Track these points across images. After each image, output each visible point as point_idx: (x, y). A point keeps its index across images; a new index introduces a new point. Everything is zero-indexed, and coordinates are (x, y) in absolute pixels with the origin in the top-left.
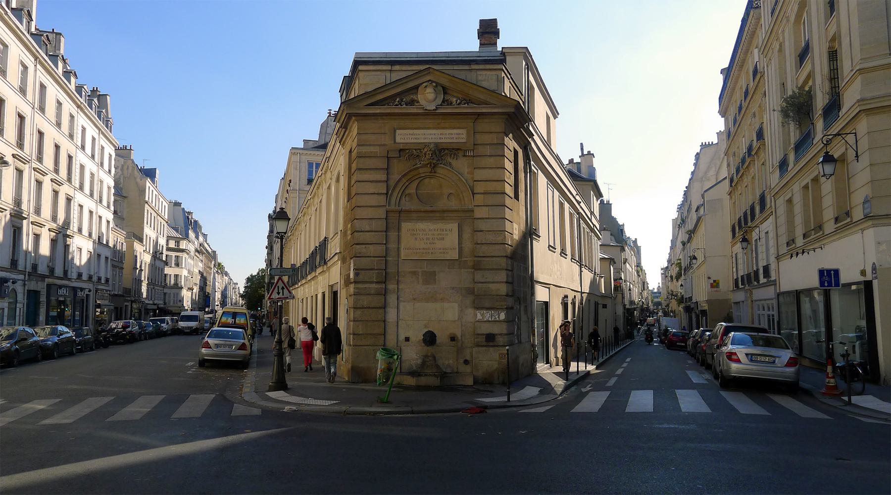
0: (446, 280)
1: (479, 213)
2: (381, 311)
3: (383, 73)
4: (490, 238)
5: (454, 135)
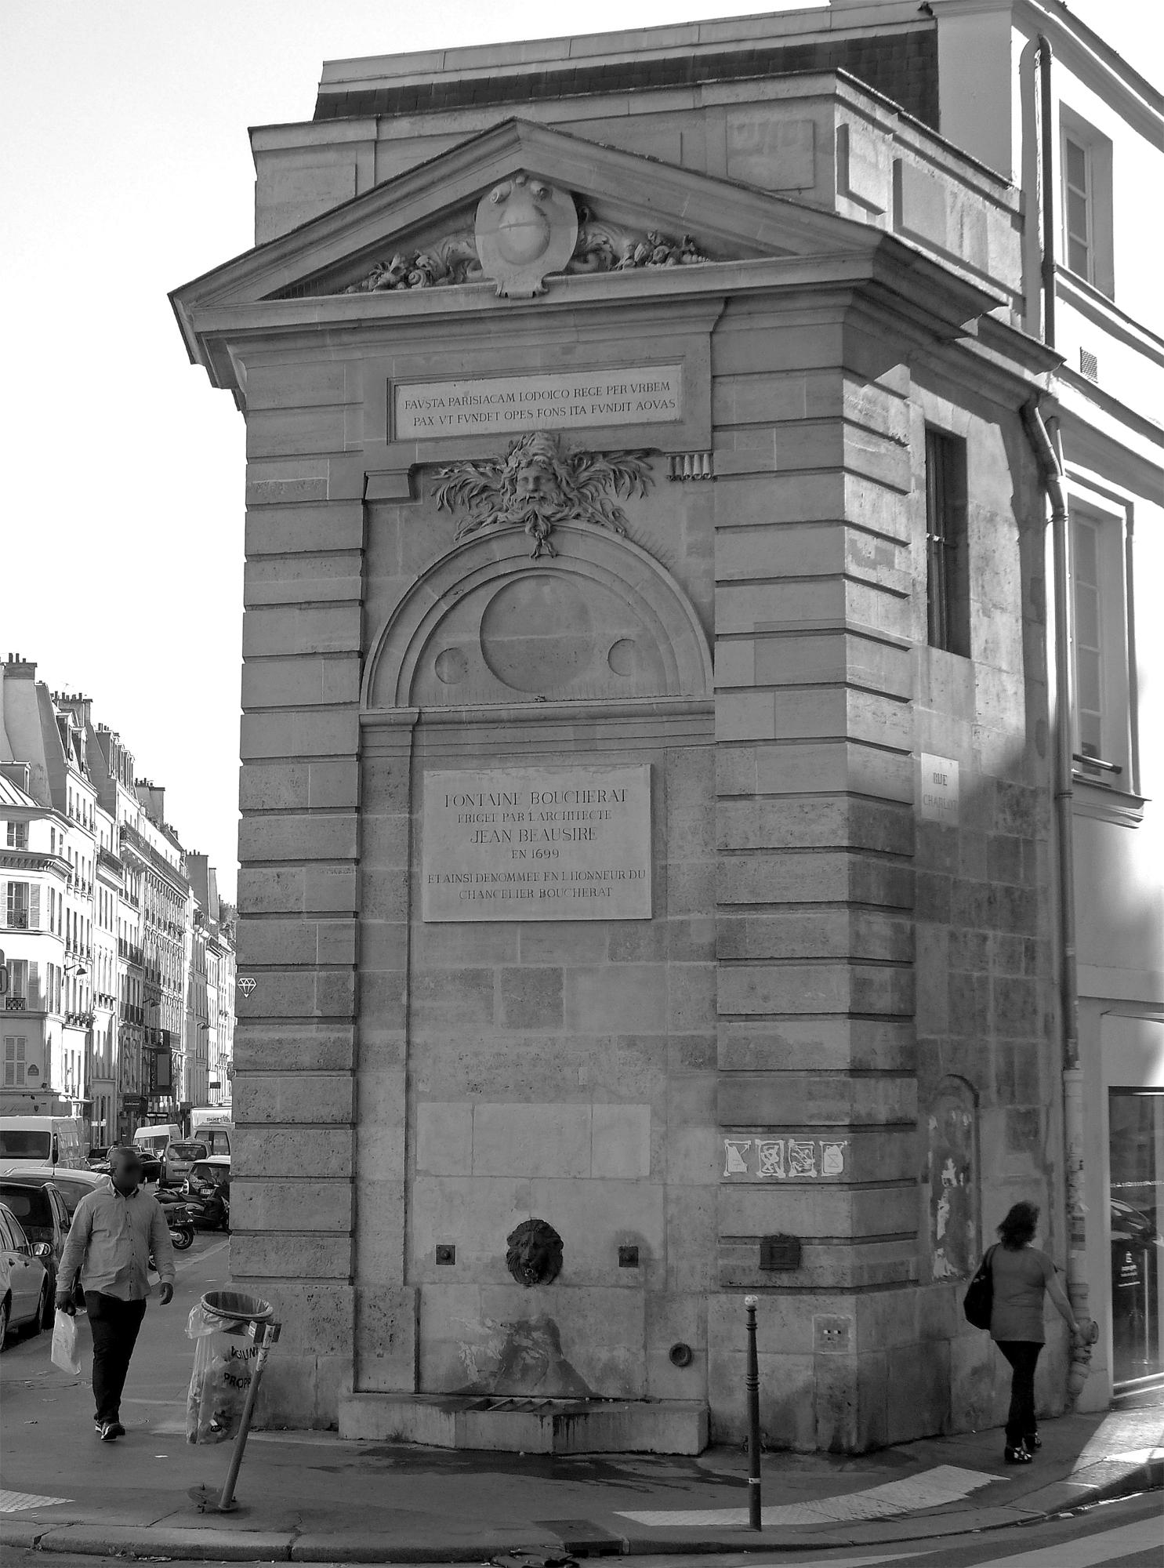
2: (343, 1137)
3: (350, 156)
5: (625, 392)
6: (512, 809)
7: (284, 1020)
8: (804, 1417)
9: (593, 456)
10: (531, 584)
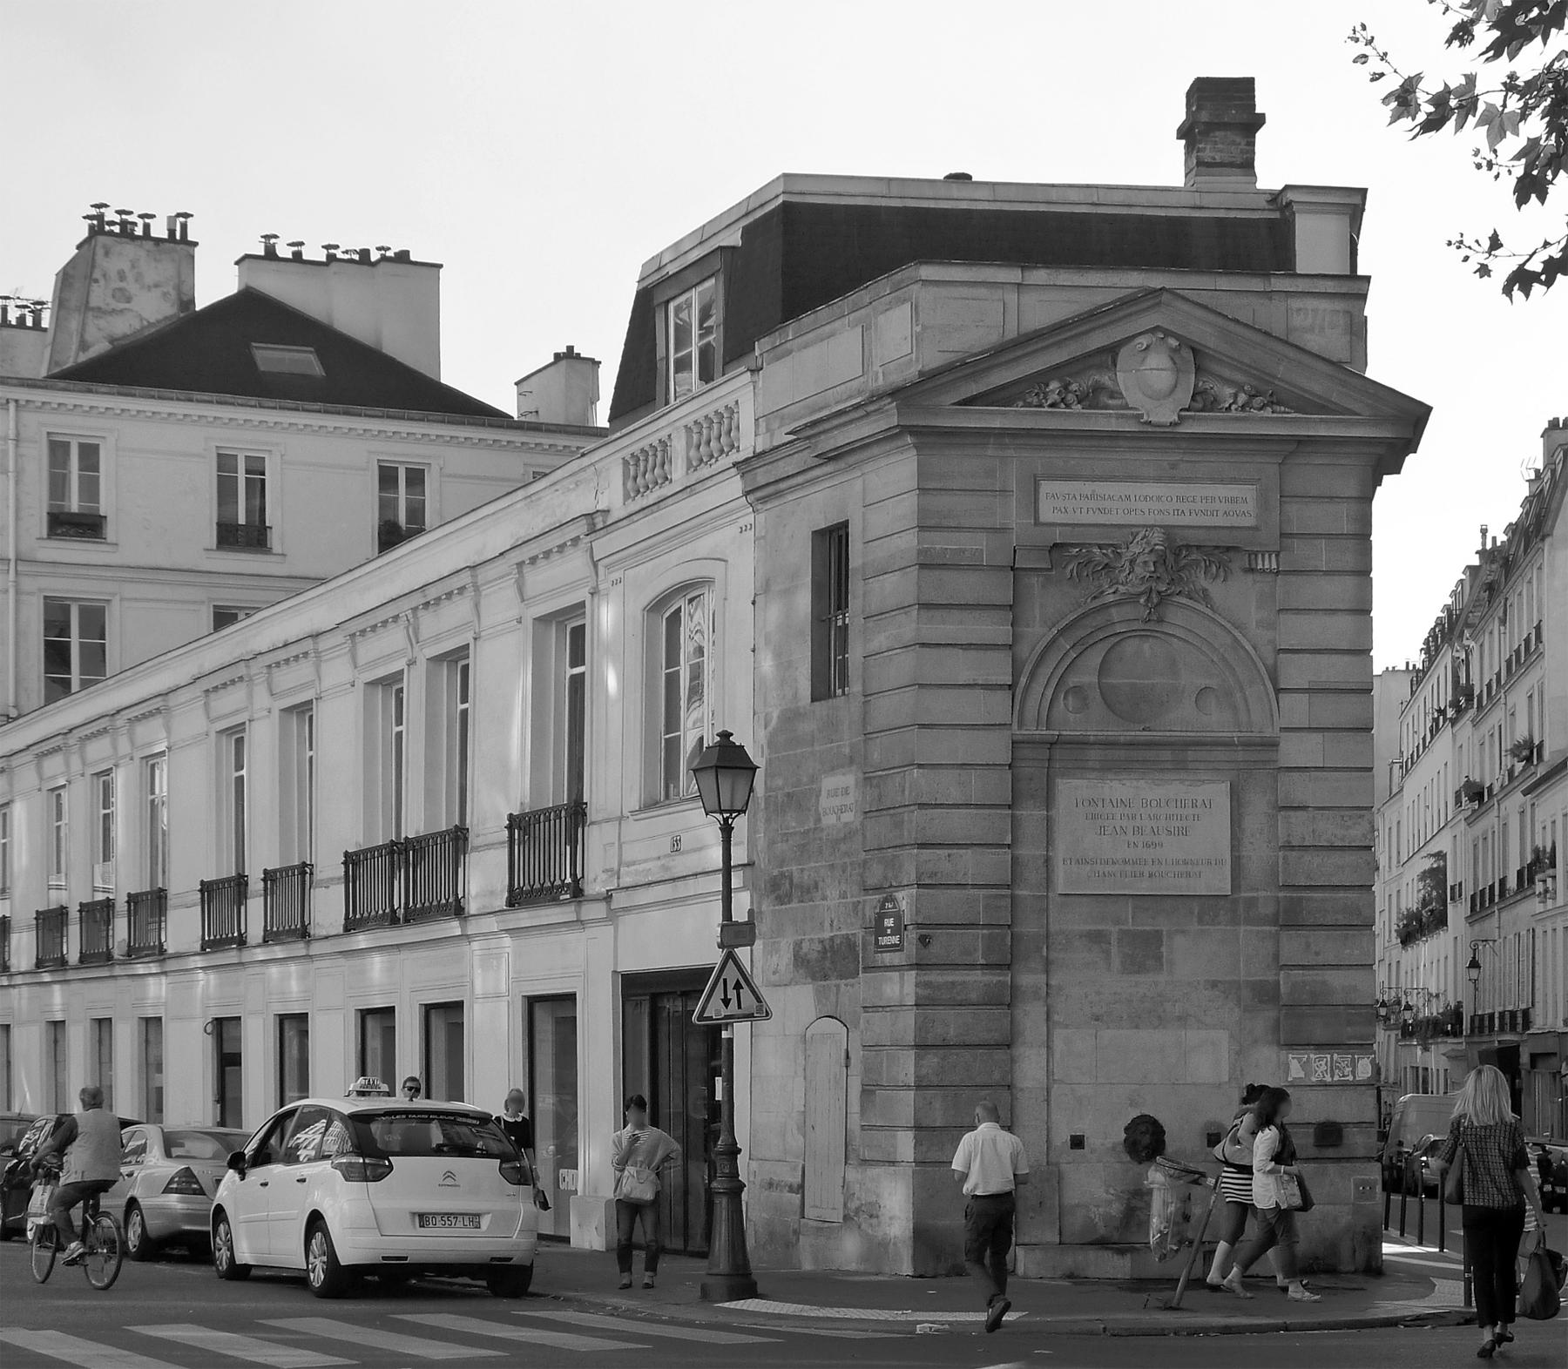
0: (1193, 957)
1: (1296, 751)
2: (999, 1055)
4: (1329, 830)
5: (1216, 502)
6: (1127, 811)
7: (955, 966)
8: (1345, 1252)
9: (1188, 547)
10: (1136, 641)
